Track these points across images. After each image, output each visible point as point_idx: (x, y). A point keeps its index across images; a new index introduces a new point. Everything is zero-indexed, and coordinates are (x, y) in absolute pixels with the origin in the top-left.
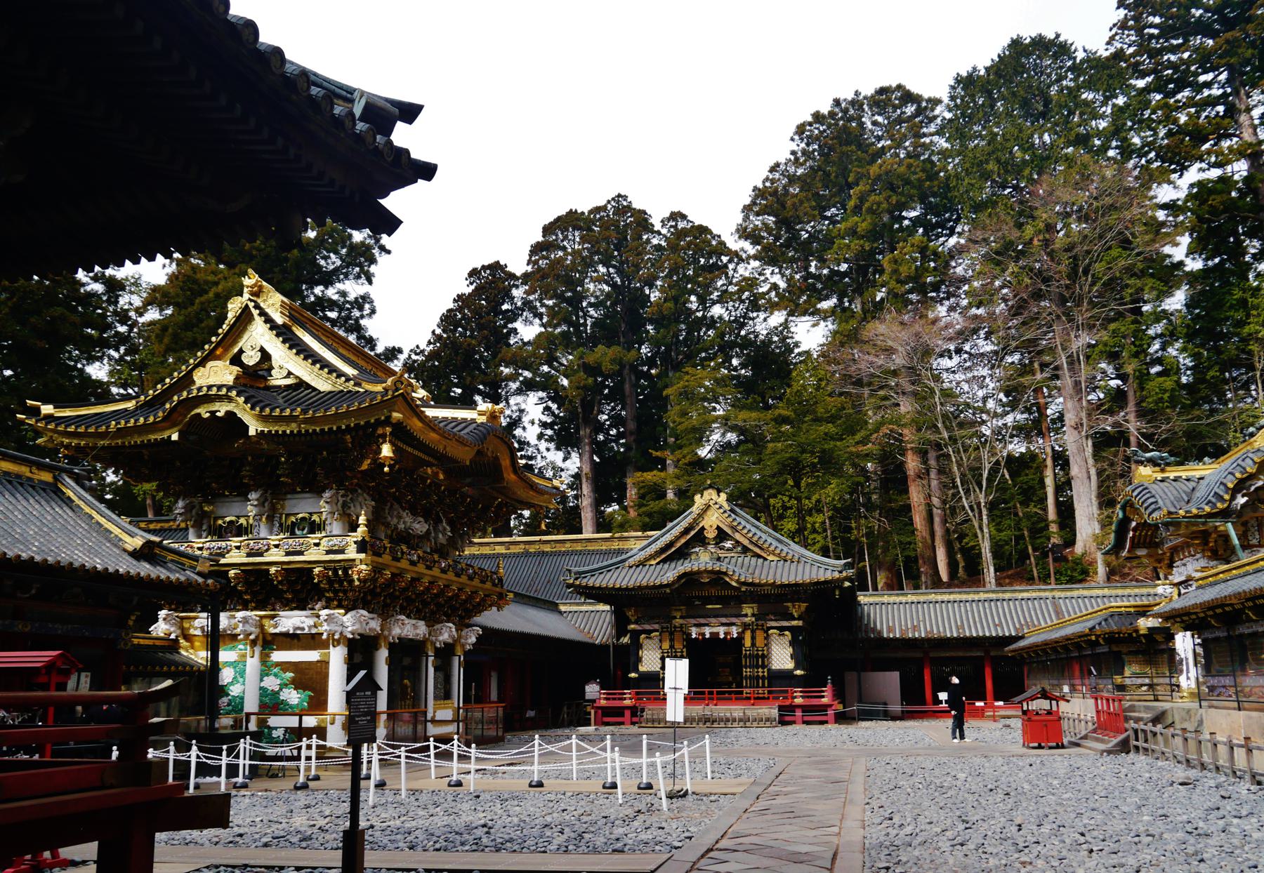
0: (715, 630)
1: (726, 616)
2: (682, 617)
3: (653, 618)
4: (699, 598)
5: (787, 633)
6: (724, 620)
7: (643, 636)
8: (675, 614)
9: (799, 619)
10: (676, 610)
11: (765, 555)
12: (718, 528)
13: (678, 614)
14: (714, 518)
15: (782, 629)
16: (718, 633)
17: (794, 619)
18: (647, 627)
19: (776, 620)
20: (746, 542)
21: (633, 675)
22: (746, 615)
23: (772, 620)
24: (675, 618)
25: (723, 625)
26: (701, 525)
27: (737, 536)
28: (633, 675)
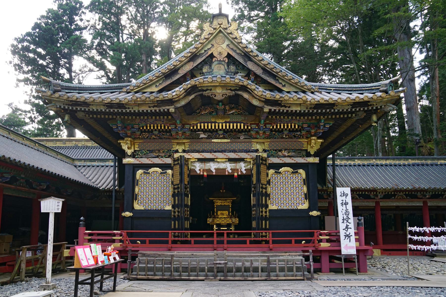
0: (222, 166)
1: (234, 151)
2: (184, 151)
3: (151, 151)
4: (204, 131)
5: (301, 171)
6: (232, 155)
7: (140, 172)
8: (176, 147)
9: (315, 155)
10: (178, 144)
11: (280, 86)
12: (229, 56)
13: (180, 148)
14: (224, 46)
15: (295, 167)
16: (224, 170)
17: (308, 155)
18: (145, 161)
19: (288, 156)
20: (259, 72)
21: (128, 214)
22: (257, 151)
23: (285, 156)
24: (177, 151)
25: (231, 160)
26: (210, 53)
27: (250, 65)
28: (128, 214)
